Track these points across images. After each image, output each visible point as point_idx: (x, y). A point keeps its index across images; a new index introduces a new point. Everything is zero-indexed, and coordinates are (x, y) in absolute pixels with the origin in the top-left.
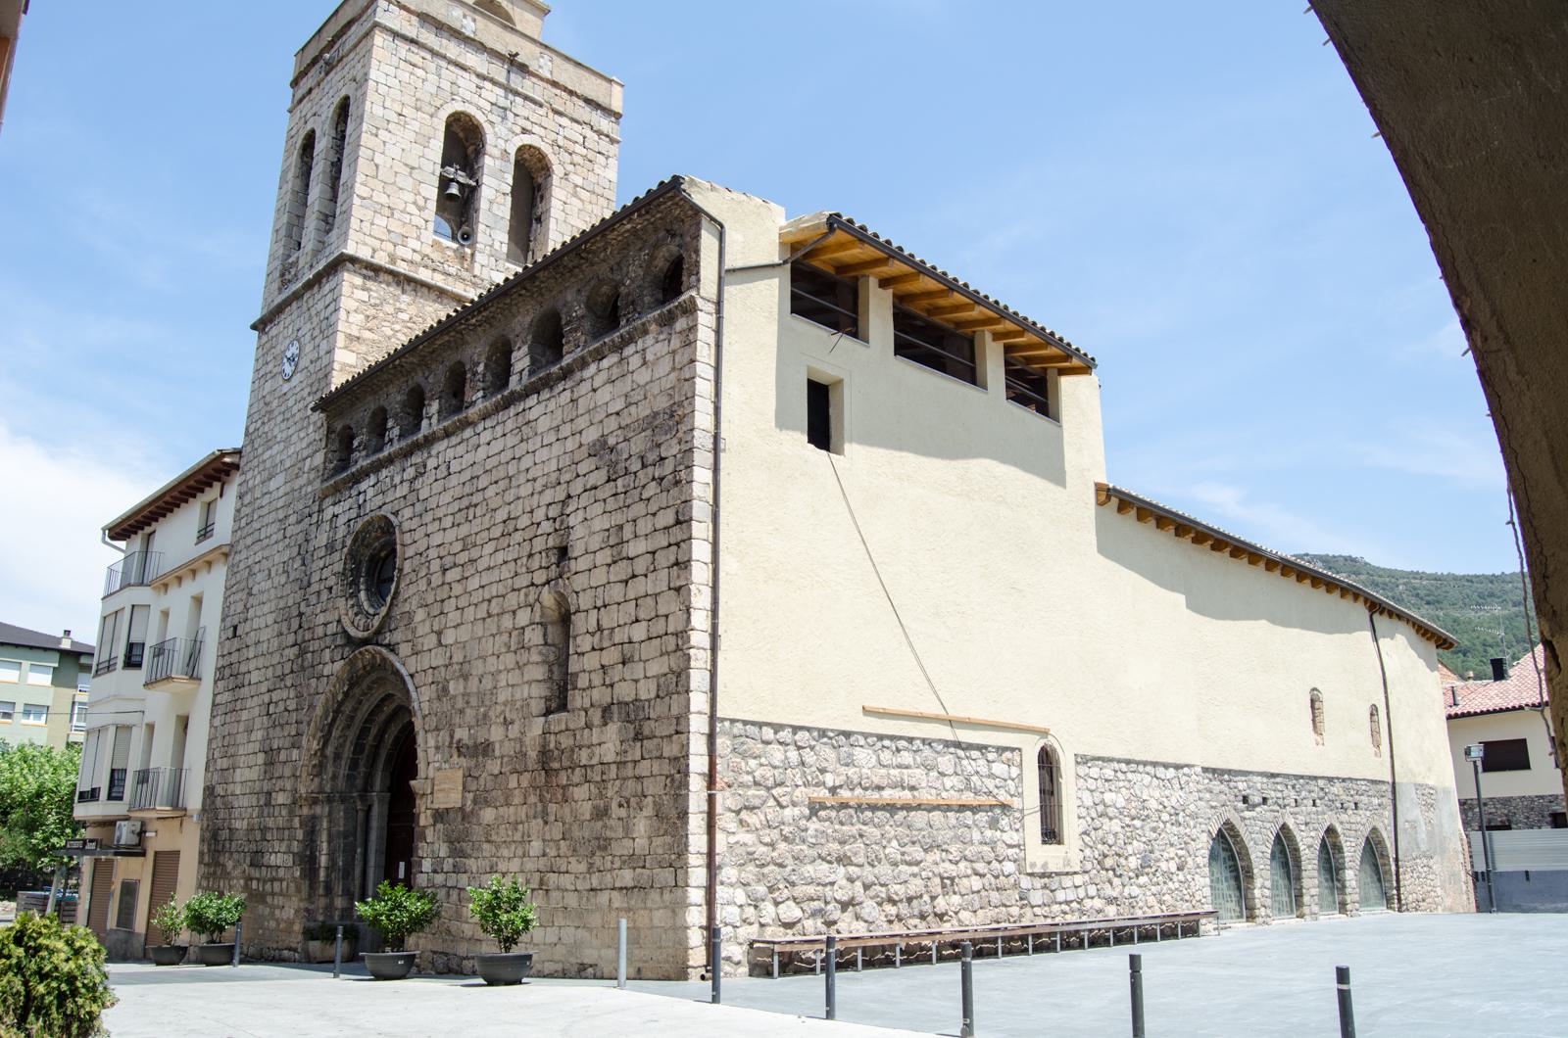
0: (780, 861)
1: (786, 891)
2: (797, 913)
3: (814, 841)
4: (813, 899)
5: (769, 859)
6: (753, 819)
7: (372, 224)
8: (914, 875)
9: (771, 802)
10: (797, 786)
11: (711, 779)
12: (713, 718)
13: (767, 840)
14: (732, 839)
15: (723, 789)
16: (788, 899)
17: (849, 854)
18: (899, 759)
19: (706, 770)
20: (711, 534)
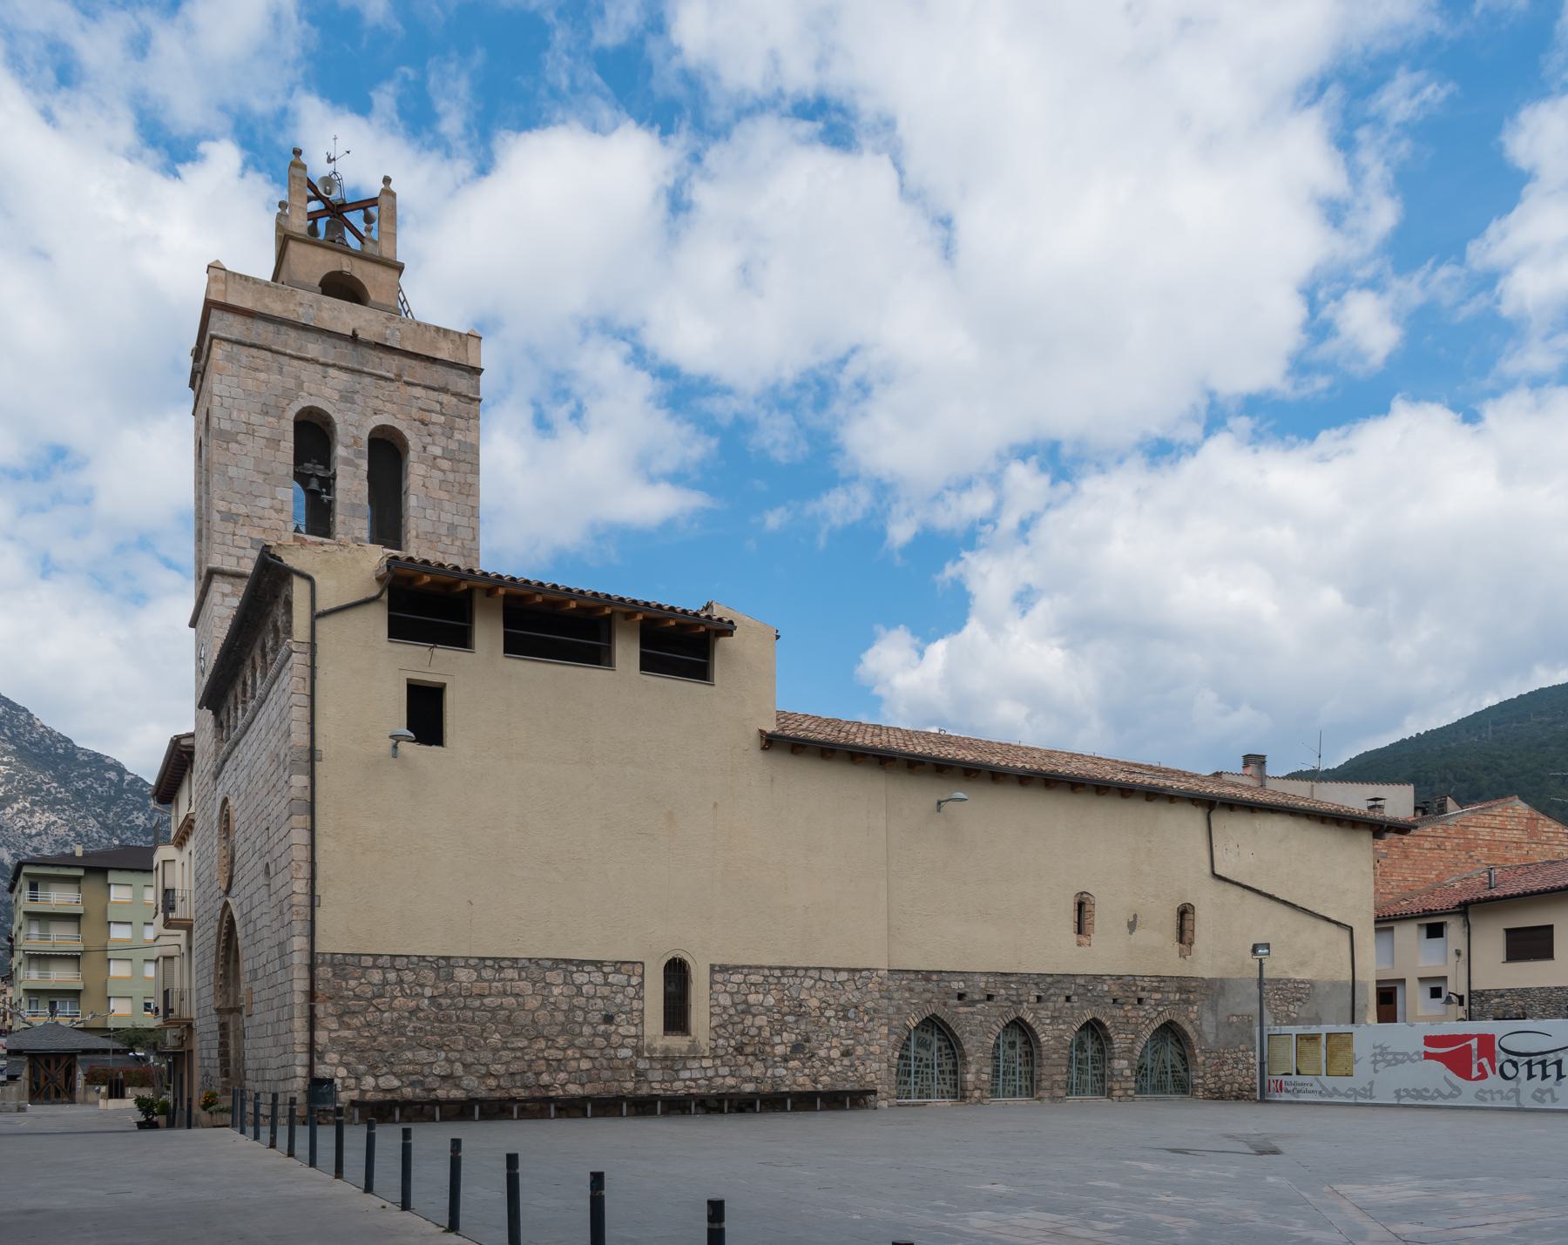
0: (380, 1048)
1: (385, 1068)
2: (396, 1083)
3: (412, 1034)
4: (411, 1074)
5: (369, 1046)
6: (356, 1022)
7: (234, 535)
8: (516, 1058)
9: (372, 1009)
10: (396, 997)
11: (312, 995)
12: (312, 954)
13: (366, 1034)
14: (333, 1035)
15: (324, 1001)
16: (386, 1073)
17: (448, 1043)
18: (502, 975)
19: (307, 988)
20: (309, 824)
